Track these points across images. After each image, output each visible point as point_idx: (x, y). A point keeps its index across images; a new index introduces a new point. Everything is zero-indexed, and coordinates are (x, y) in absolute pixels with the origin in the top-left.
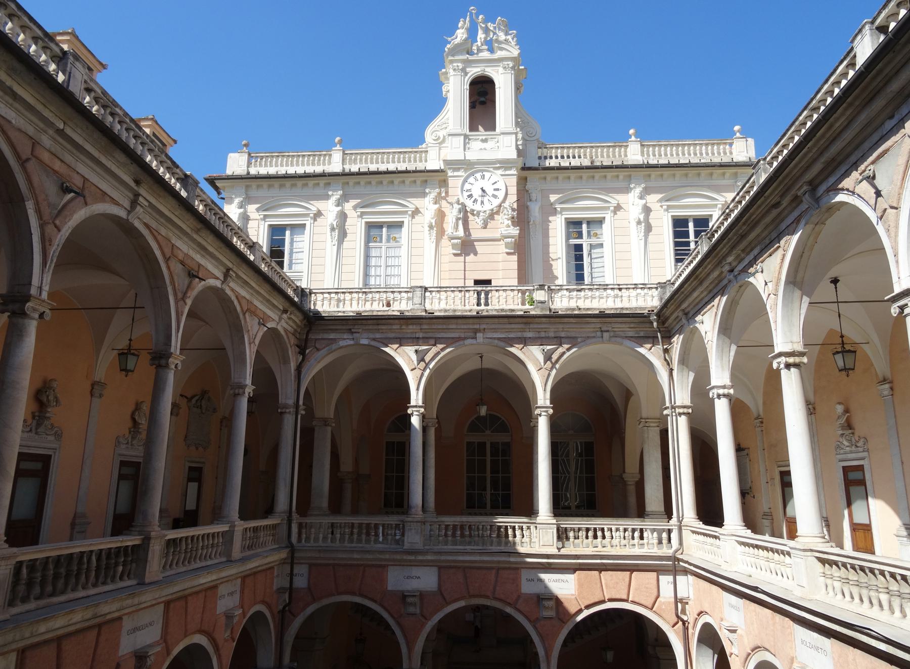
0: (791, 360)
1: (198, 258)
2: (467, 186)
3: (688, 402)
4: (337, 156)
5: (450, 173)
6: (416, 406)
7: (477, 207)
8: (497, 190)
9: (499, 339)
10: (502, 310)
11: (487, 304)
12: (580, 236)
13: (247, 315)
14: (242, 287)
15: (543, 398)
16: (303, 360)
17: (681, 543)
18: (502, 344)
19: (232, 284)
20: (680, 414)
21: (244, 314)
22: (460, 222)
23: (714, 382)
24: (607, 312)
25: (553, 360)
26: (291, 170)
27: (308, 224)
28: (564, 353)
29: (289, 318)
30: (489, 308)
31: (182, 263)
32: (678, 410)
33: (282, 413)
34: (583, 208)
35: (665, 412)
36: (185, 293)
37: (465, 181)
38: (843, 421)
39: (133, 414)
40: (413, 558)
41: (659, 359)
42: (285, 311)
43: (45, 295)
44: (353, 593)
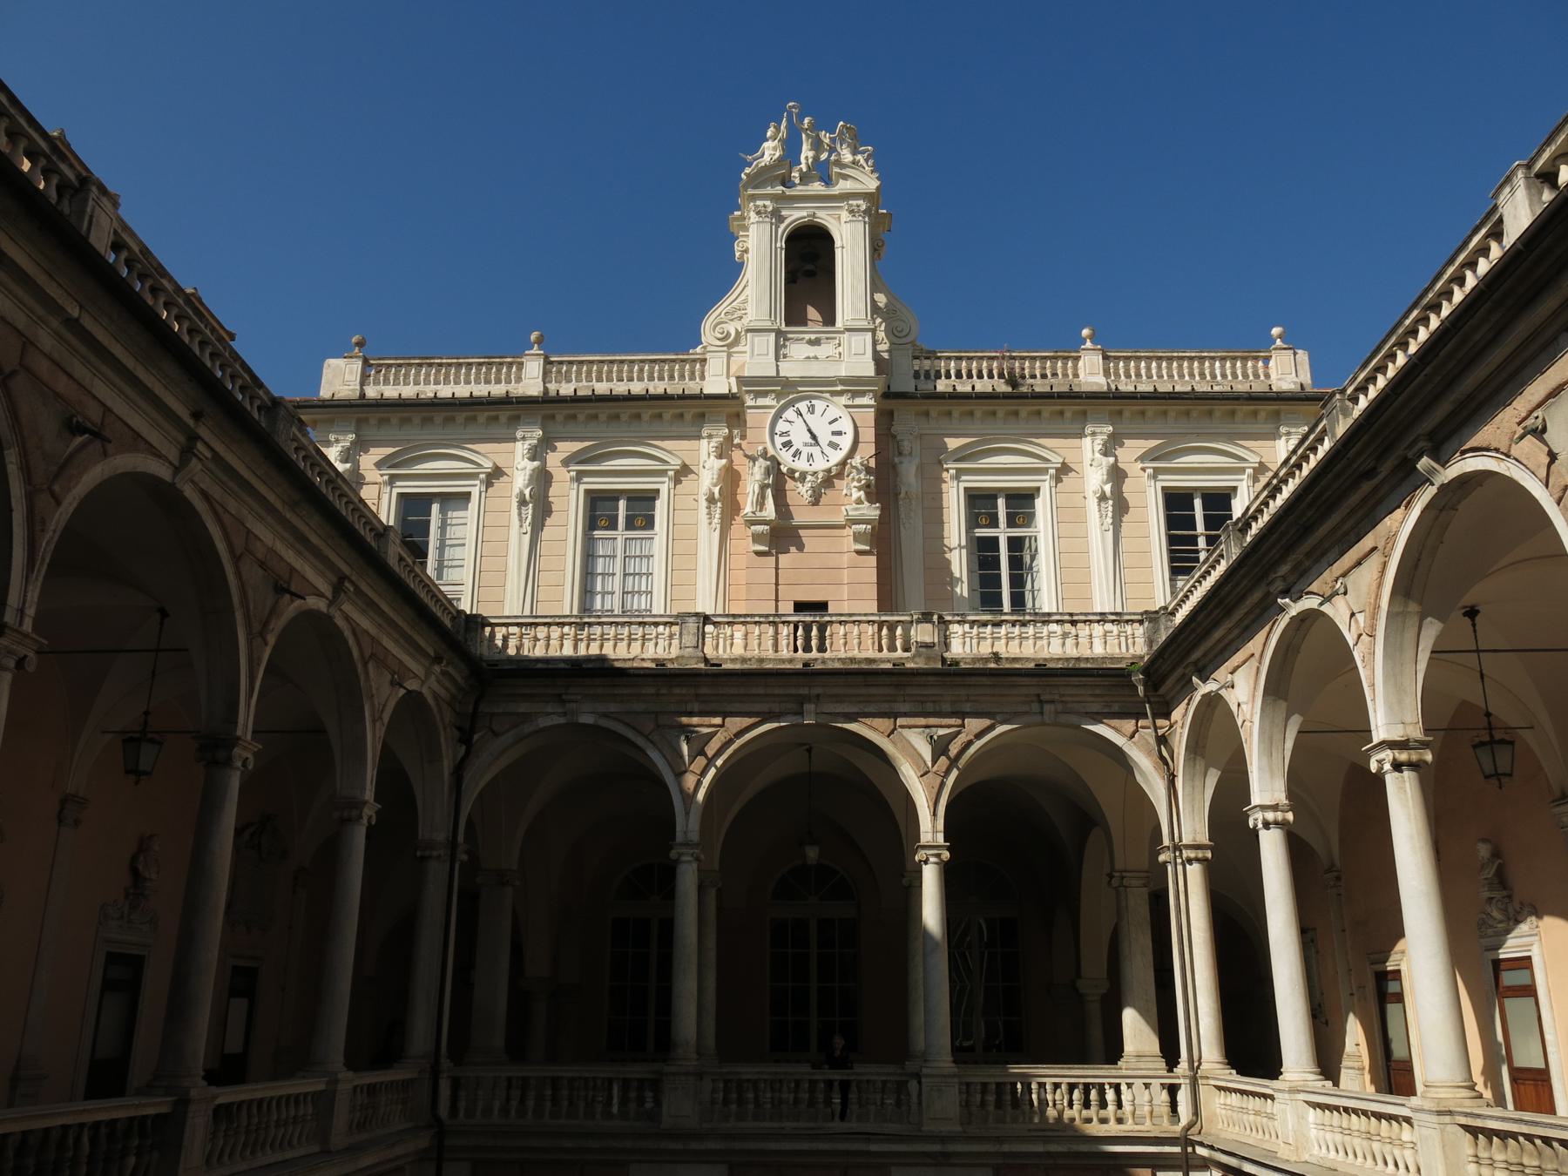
0: (1403, 756)
1: (290, 556)
2: (781, 426)
3: (1204, 838)
4: (533, 368)
5: (749, 402)
6: (687, 844)
7: (801, 465)
8: (839, 433)
10: (852, 660)
11: (822, 649)
12: (994, 523)
13: (371, 666)
14: (363, 612)
15: (930, 828)
16: (467, 754)
17: (1196, 1111)
19: (346, 607)
20: (1190, 861)
21: (365, 664)
22: (769, 492)
23: (1256, 798)
24: (1050, 665)
26: (445, 391)
27: (475, 492)
29: (444, 673)
30: (827, 655)
31: (262, 564)
32: (1186, 854)
33: (422, 858)
34: (1002, 468)
35: (1162, 858)
36: (266, 624)
37: (778, 416)
38: (1490, 873)
39: (134, 858)
40: (679, 1146)
41: (1149, 754)
42: (438, 659)
43: (28, 625)
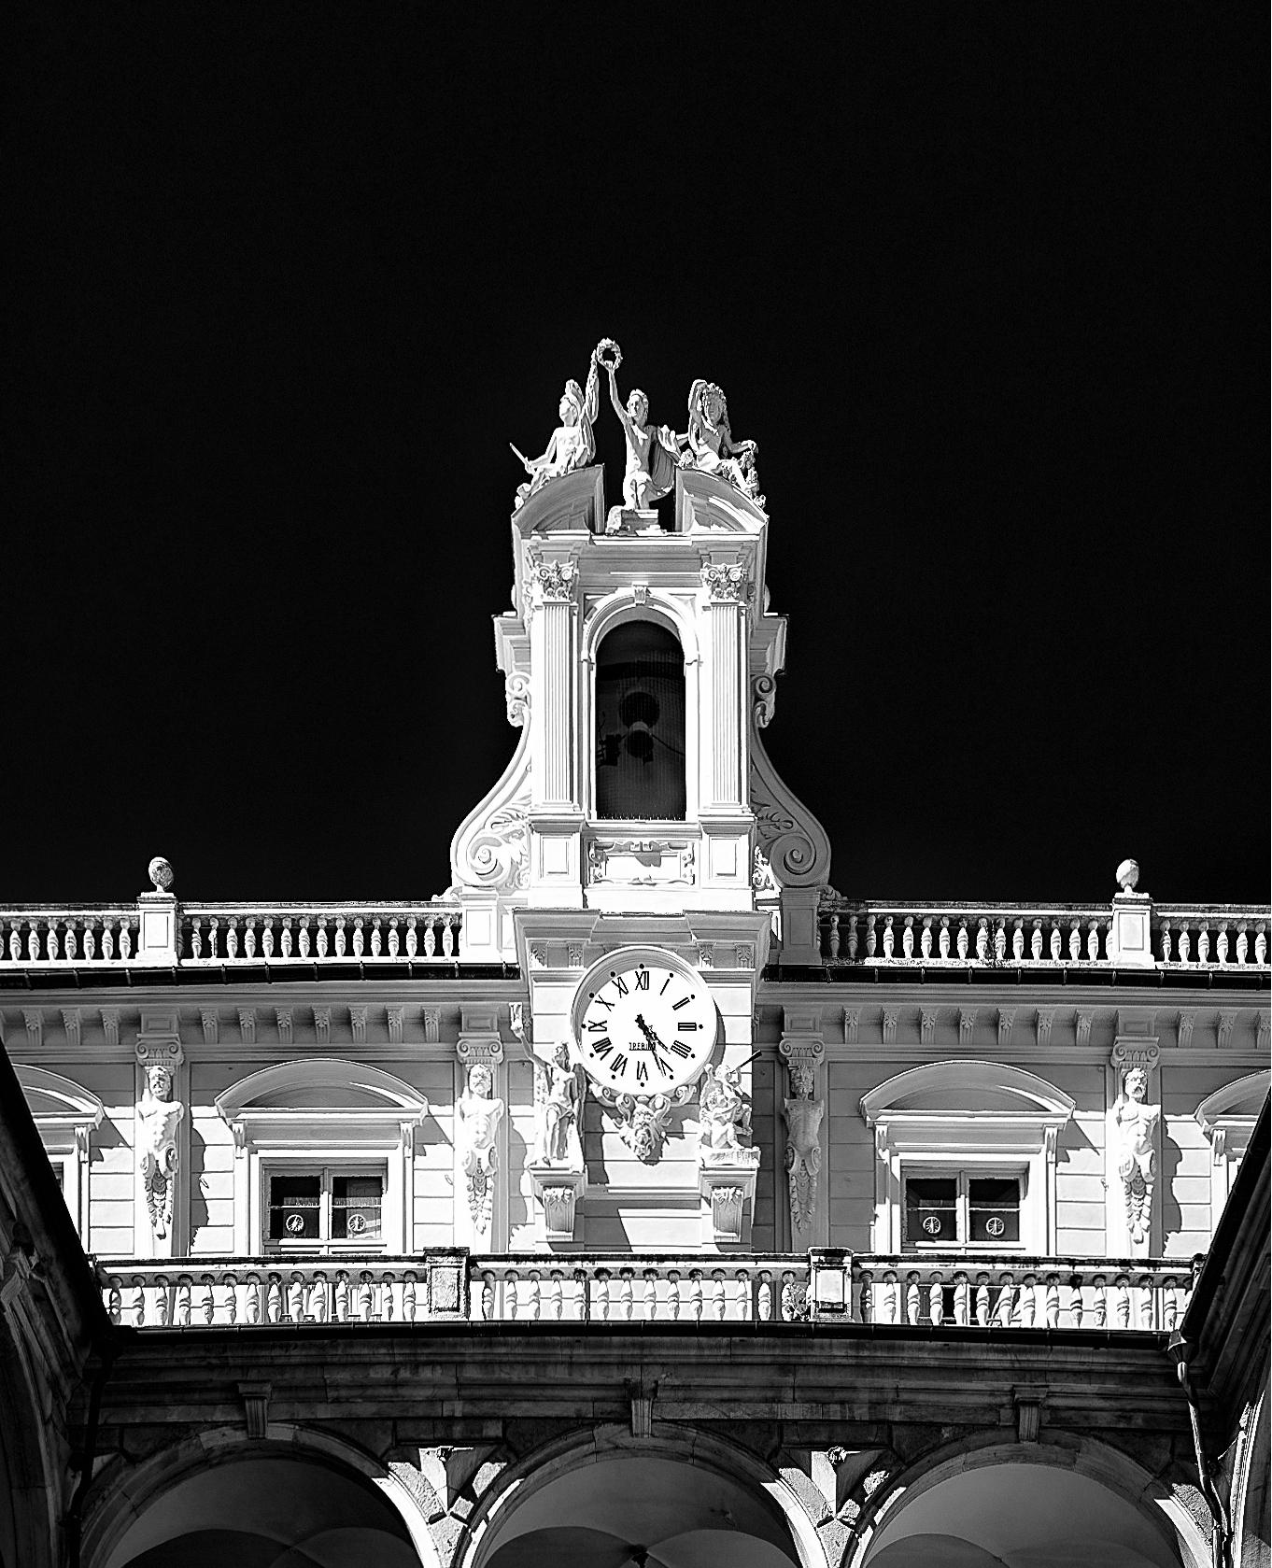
2: (594, 1013)
8: (691, 1027)
9: (699, 1424)
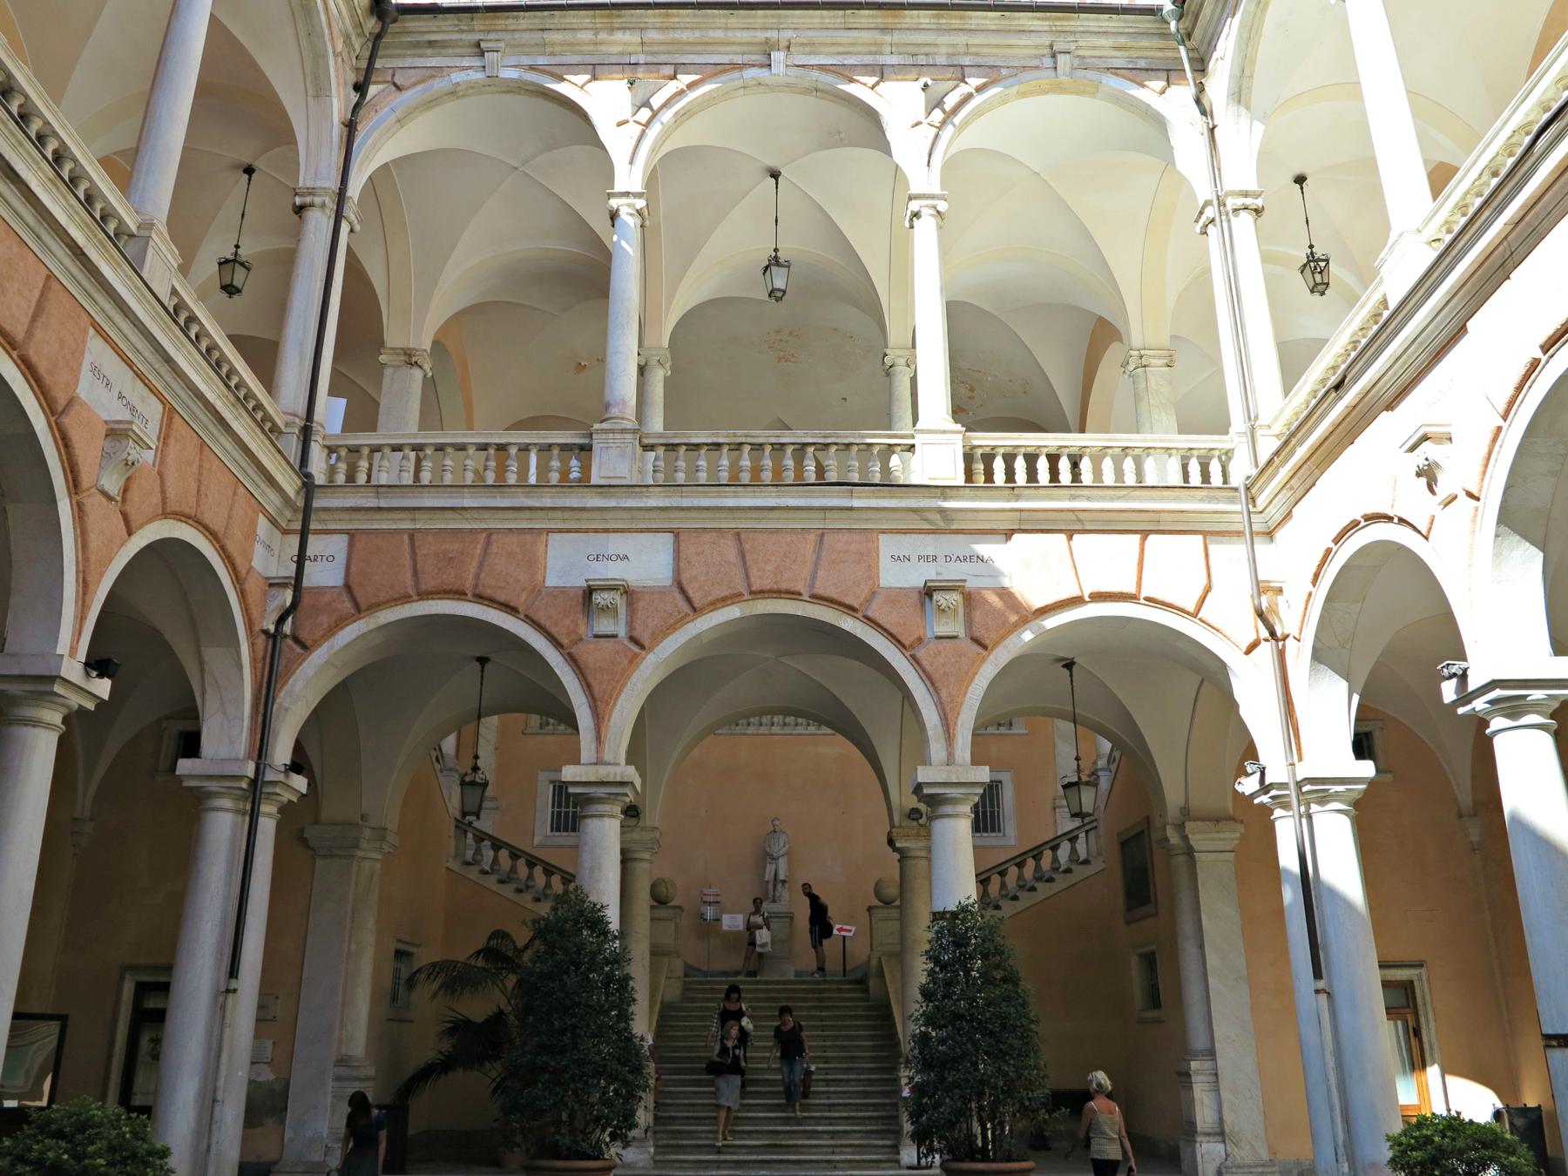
6: (627, 194)
9: (822, 67)
18: (827, 79)
25: (948, 107)
28: (969, 97)
32: (1231, 203)
44: (458, 594)
